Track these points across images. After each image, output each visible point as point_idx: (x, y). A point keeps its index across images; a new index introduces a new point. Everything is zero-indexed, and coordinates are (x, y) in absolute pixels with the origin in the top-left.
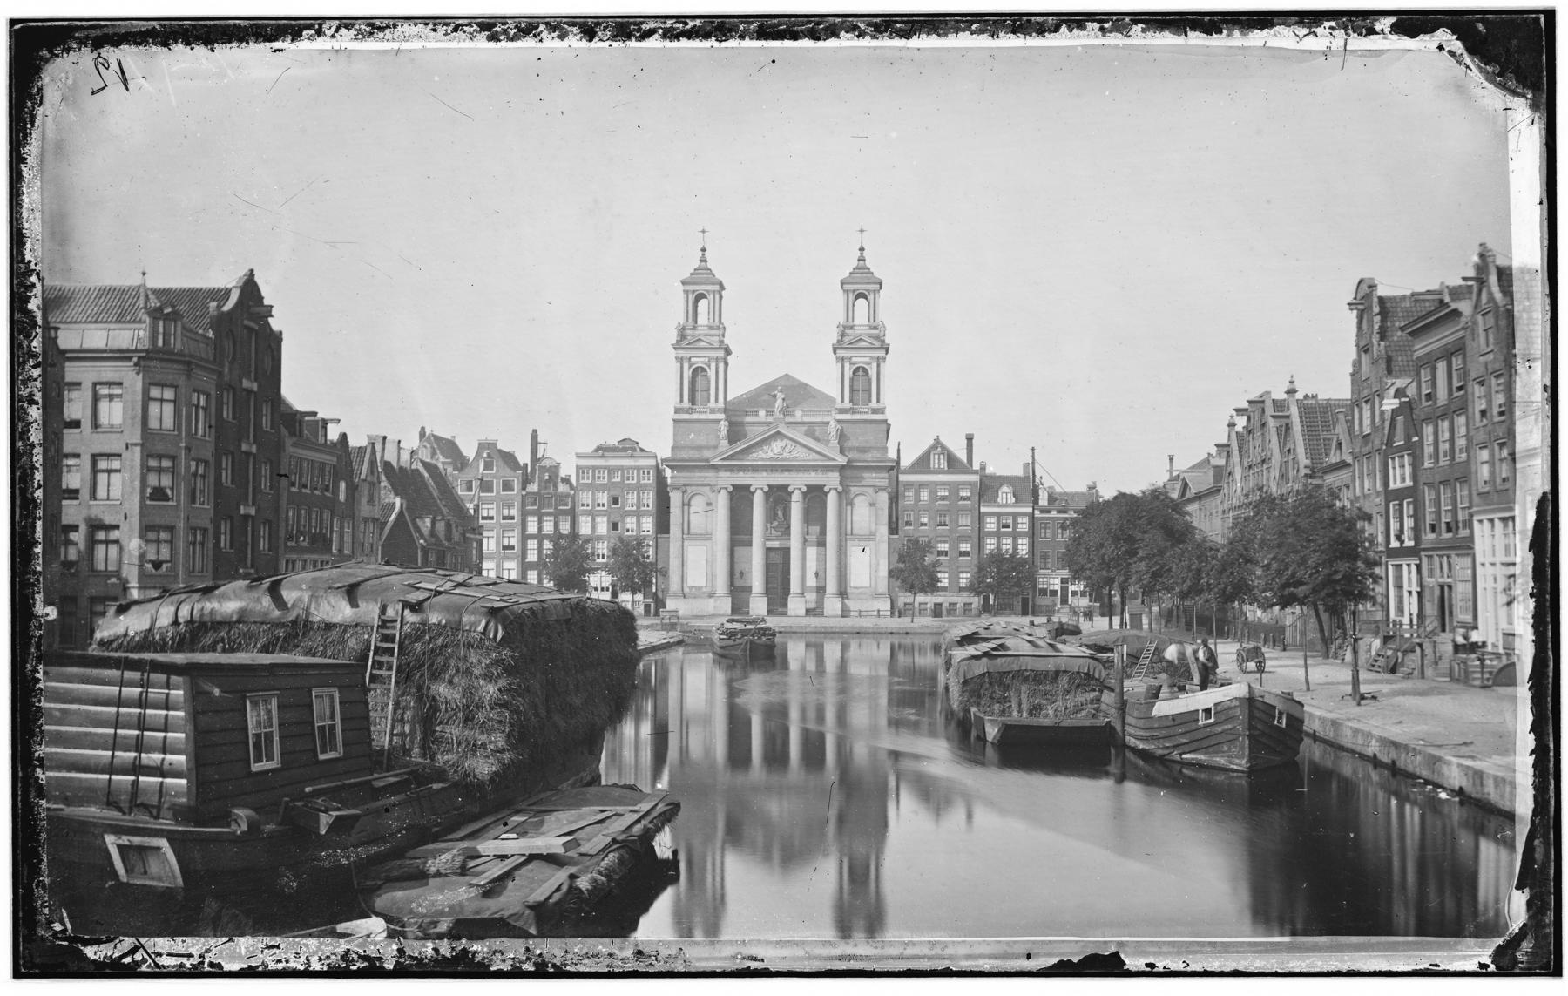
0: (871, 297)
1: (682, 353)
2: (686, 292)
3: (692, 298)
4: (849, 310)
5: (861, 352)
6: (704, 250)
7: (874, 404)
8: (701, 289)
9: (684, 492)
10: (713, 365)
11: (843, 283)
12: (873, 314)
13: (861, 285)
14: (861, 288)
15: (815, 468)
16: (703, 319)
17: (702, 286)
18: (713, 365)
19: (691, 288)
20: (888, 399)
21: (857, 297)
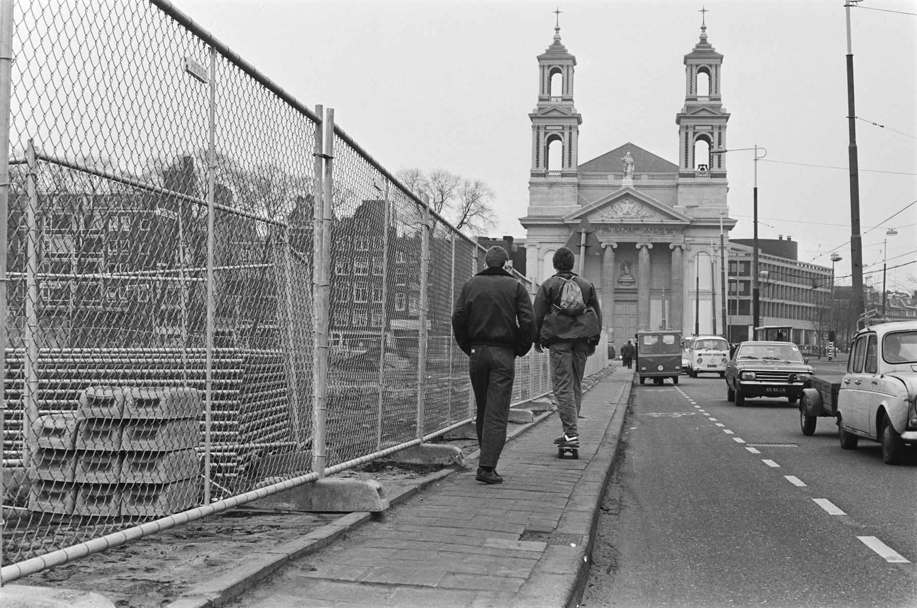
0: (712, 71)
1: (538, 122)
2: (542, 67)
3: (547, 72)
4: (692, 85)
5: (702, 121)
6: (557, 29)
7: (715, 169)
8: (556, 63)
10: (567, 134)
11: (686, 58)
12: (714, 85)
13: (704, 60)
14: (704, 63)
15: (660, 228)
16: (557, 89)
17: (556, 61)
19: (546, 63)
20: (727, 167)
21: (699, 71)
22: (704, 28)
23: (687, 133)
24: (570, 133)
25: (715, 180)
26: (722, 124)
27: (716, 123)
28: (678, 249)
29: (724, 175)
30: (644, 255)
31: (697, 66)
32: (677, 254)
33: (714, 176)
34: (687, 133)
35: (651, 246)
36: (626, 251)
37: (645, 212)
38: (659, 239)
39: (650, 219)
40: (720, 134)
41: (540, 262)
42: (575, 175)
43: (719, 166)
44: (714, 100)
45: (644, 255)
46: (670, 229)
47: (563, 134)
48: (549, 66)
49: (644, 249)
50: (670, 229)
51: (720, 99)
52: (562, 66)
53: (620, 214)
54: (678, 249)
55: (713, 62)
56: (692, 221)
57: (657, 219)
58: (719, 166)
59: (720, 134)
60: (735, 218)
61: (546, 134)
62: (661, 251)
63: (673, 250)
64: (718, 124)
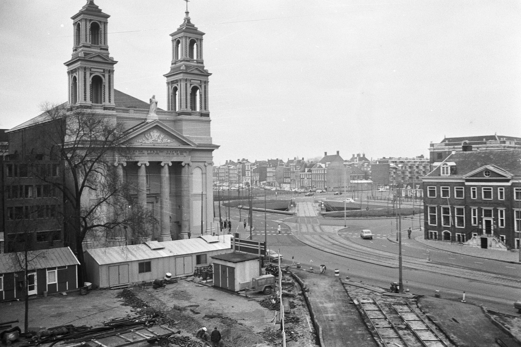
10: (107, 75)
18: (107, 75)
22: (187, 13)
23: (186, 84)
25: (204, 118)
26: (206, 80)
27: (203, 79)
28: (187, 165)
29: (208, 115)
31: (189, 38)
33: (202, 115)
34: (186, 84)
35: (171, 164)
36: (155, 167)
38: (175, 159)
39: (172, 144)
40: (205, 86)
42: (113, 109)
43: (205, 109)
44: (200, 63)
46: (182, 151)
48: (90, 20)
49: (166, 166)
50: (182, 151)
51: (202, 63)
52: (100, 22)
53: (151, 141)
55: (199, 37)
56: (198, 146)
57: (175, 145)
58: (205, 109)
59: (205, 86)
60: (218, 144)
61: (91, 74)
62: (177, 168)
63: (184, 167)
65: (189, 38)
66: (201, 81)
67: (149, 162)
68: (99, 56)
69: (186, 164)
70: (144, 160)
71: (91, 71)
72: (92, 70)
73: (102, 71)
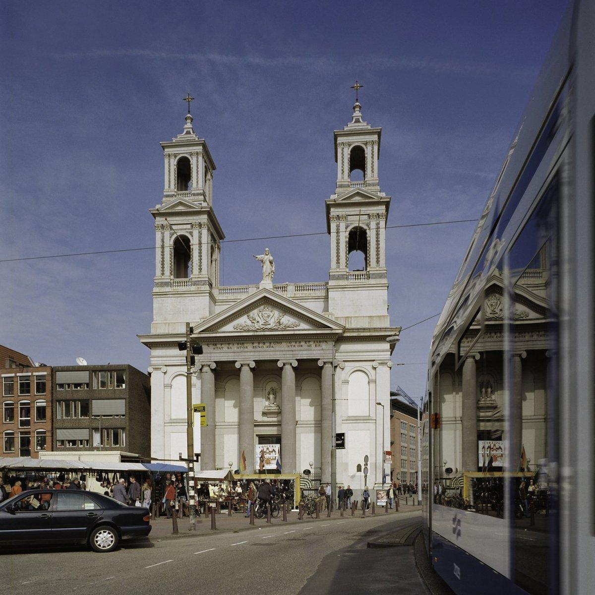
9: (165, 373)
10: (196, 233)
24: (200, 233)
28: (328, 366)
30: (289, 375)
32: (327, 370)
35: (295, 364)
36: (266, 372)
37: (287, 320)
41: (167, 390)
45: (289, 375)
47: (191, 233)
52: (191, 154)
54: (328, 366)
61: (172, 235)
62: (309, 371)
64: (375, 212)
65: (350, 145)
66: (369, 214)
67: (254, 361)
68: (180, 204)
69: (325, 363)
70: (245, 357)
71: (171, 229)
72: (174, 227)
73: (189, 226)
